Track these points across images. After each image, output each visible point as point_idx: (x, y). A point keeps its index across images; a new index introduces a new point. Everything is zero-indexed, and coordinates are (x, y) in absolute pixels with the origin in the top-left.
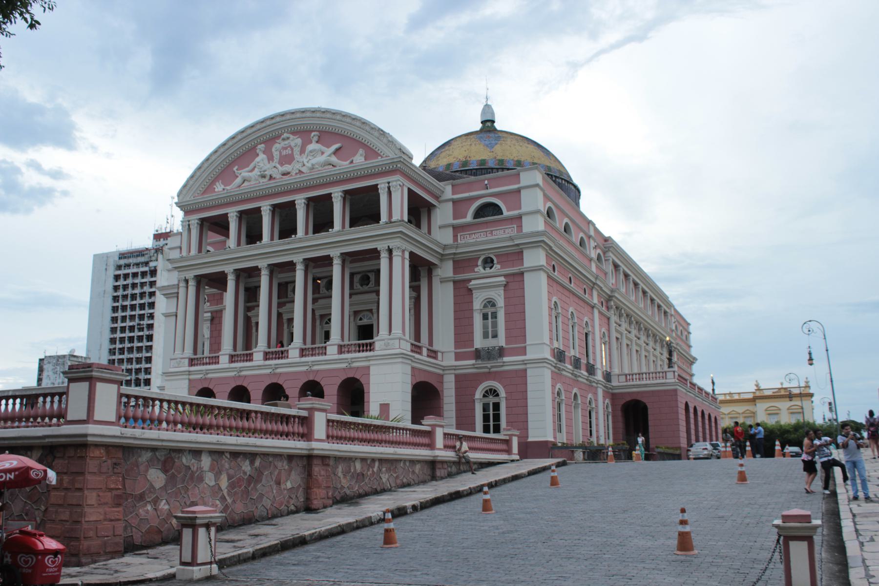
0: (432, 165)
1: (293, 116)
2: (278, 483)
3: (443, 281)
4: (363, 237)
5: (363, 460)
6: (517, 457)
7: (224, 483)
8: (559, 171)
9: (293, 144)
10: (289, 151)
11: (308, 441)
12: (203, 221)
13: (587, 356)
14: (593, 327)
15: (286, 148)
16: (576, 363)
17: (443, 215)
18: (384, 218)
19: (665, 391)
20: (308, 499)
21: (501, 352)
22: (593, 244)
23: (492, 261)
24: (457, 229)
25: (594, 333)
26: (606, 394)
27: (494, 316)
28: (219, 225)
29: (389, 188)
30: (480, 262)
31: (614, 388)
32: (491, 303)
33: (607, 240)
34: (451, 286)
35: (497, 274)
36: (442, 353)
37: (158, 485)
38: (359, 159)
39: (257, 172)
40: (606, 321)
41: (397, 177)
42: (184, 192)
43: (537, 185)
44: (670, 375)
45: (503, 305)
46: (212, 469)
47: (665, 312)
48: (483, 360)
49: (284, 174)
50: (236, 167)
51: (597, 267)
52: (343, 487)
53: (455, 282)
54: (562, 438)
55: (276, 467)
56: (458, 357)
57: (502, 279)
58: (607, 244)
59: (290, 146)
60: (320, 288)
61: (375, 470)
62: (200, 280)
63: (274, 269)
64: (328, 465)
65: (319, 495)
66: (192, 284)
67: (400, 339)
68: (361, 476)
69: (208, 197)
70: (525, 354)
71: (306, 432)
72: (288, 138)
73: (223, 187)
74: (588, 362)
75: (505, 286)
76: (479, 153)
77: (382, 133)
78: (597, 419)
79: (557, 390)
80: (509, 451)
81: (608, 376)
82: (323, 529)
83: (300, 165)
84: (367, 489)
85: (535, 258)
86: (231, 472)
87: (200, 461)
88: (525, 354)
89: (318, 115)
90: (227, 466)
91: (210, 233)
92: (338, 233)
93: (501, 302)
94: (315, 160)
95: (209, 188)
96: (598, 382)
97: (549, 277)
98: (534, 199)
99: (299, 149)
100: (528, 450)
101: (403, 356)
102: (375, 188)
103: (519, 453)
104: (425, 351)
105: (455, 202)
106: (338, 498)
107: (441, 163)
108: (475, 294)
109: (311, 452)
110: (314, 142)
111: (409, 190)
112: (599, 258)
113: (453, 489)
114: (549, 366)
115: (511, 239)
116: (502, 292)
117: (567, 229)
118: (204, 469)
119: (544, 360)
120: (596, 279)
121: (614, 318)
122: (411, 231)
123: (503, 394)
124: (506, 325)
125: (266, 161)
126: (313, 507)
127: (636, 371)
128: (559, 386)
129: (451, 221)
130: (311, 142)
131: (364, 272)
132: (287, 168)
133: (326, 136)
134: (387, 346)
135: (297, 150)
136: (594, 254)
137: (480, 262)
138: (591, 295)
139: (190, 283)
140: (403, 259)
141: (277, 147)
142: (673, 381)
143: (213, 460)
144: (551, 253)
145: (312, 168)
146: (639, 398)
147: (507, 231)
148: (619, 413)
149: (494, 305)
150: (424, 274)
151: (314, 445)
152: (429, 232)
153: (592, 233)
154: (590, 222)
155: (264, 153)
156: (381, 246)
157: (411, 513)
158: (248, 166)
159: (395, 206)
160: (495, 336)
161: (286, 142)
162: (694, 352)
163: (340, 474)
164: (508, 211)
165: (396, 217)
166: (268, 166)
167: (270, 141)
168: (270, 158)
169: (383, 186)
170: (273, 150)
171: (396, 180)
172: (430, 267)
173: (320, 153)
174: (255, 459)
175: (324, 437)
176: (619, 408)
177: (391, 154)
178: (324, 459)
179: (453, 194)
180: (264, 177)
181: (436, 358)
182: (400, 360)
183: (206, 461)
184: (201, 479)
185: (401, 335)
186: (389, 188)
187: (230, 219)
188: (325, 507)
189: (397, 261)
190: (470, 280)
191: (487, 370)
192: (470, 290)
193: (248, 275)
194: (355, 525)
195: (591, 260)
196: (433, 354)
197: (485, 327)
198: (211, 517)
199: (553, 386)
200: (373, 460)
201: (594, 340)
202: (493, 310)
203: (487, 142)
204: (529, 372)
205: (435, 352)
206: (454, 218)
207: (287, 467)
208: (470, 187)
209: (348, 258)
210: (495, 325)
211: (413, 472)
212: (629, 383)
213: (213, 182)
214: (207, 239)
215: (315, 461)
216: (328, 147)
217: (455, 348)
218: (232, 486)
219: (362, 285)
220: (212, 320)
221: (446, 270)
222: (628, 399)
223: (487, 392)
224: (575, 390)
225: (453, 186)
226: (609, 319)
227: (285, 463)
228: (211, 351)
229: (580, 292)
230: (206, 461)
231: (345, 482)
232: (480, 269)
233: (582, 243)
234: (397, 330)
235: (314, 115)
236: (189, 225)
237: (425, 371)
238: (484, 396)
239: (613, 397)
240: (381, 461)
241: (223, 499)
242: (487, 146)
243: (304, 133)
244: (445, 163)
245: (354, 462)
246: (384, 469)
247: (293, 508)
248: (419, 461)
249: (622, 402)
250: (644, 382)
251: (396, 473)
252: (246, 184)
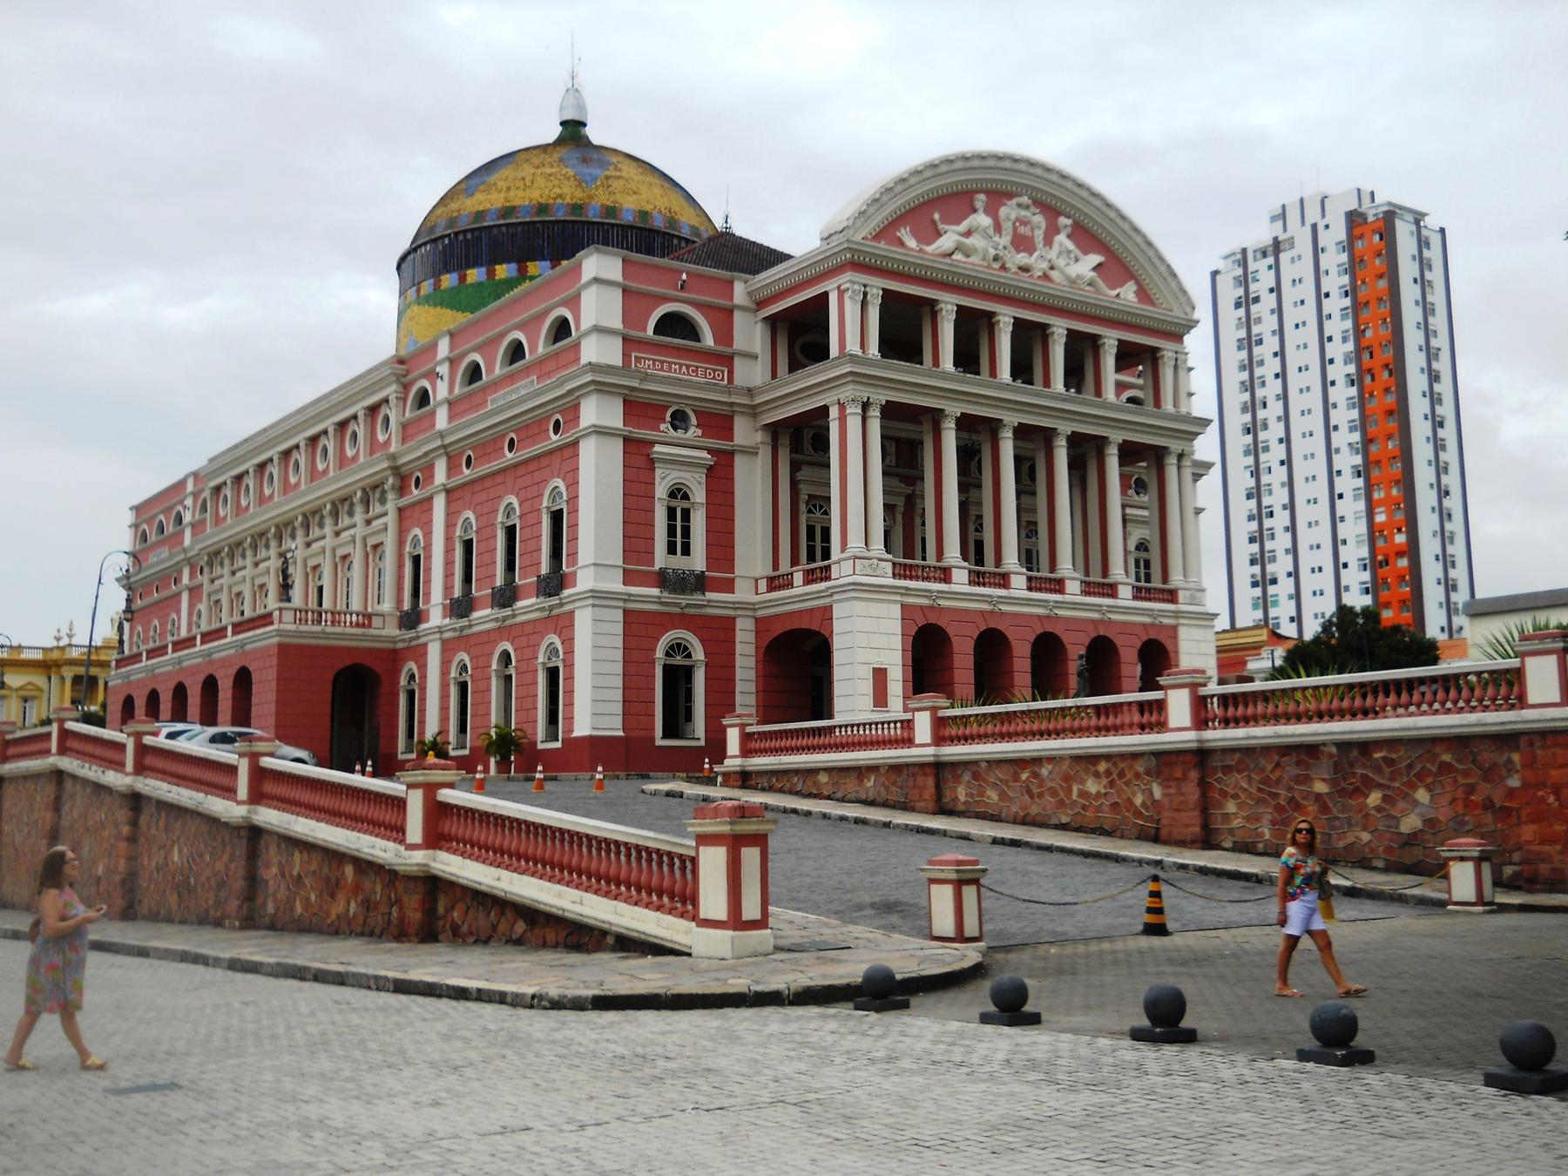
1: (1062, 182)
15: (1025, 223)
38: (1128, 292)
66: (875, 413)
72: (1027, 207)
73: (912, 243)
132: (1022, 258)
135: (1039, 235)
156: (1175, 446)
158: (958, 223)
167: (998, 196)
168: (998, 228)
216: (1086, 253)
236: (865, 294)
252: (958, 256)
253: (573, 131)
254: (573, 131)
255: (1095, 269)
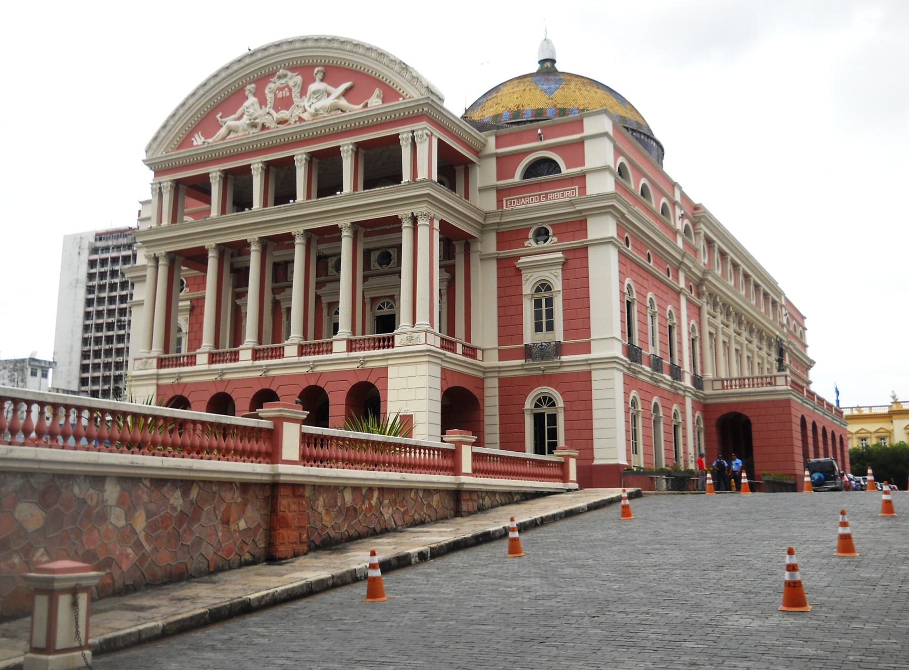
0: (476, 116)
1: (292, 46)
2: (226, 522)
3: (484, 258)
4: (379, 202)
5: (356, 489)
6: (576, 486)
7: (140, 523)
8: (638, 123)
9: (291, 84)
10: (285, 93)
11: (272, 463)
12: (177, 184)
13: (671, 355)
14: (679, 318)
15: (282, 89)
16: (656, 364)
17: (485, 174)
18: (406, 177)
19: (774, 401)
20: (271, 544)
21: (559, 349)
22: (679, 212)
23: (547, 232)
24: (502, 192)
25: (680, 326)
26: (696, 405)
27: (549, 302)
28: (197, 188)
29: (413, 138)
30: (531, 235)
31: (706, 397)
32: (544, 286)
33: (697, 208)
34: (493, 266)
35: (552, 251)
36: (483, 350)
37: (31, 527)
39: (245, 120)
40: (696, 311)
41: (424, 124)
42: (154, 146)
43: (606, 134)
44: (781, 381)
45: (560, 288)
46: (121, 503)
47: (774, 303)
48: (534, 359)
49: (282, 122)
50: (220, 114)
51: (684, 242)
52: (324, 527)
53: (499, 260)
54: (639, 461)
55: (222, 500)
56: (503, 356)
57: (560, 255)
58: (697, 214)
59: (288, 86)
60: (325, 268)
61: (373, 502)
62: (175, 259)
63: (266, 243)
64: (302, 496)
65: (287, 538)
67: (426, 332)
68: (353, 511)
69: (184, 152)
70: (589, 352)
71: (270, 450)
72: (285, 76)
73: (203, 139)
74: (672, 363)
75: (564, 264)
76: (534, 100)
77: (405, 67)
78: (685, 437)
79: (631, 398)
80: (564, 478)
81: (698, 382)
82: (279, 589)
83: (301, 110)
84: (361, 529)
85: (602, 228)
86: (152, 507)
87: (103, 491)
88: (589, 352)
89: (323, 44)
90: (145, 498)
91: (189, 200)
92: (348, 197)
93: (558, 285)
94: (320, 103)
95: (186, 141)
96: (686, 389)
97: (621, 253)
98: (600, 154)
99: (299, 90)
100: (592, 476)
101: (430, 353)
102: (395, 139)
103: (579, 480)
104: (459, 348)
105: (499, 158)
106: (318, 543)
107: (486, 114)
108: (525, 275)
109: (277, 478)
110: (317, 80)
111: (439, 140)
112: (687, 230)
113: (480, 530)
114: (621, 368)
115: (571, 203)
116: (560, 272)
117: (644, 192)
118: (109, 503)
119: (613, 360)
120: (683, 256)
121: (706, 308)
122: (442, 194)
123: (560, 403)
124: (564, 313)
125: (257, 106)
126: (278, 555)
127: (735, 375)
128: (633, 393)
129: (493, 181)
130: (314, 81)
131: (381, 247)
132: (284, 114)
133: (333, 72)
134: (410, 341)
135: (296, 92)
136: (679, 225)
137: (531, 235)
138: (677, 278)
139: (161, 262)
140: (431, 229)
141: (270, 88)
142: (784, 388)
143: (123, 490)
144: (623, 225)
145: (316, 114)
146: (739, 410)
147: (566, 194)
148: (714, 430)
149: (549, 289)
150: (459, 249)
151: (282, 468)
152: (467, 196)
153: (678, 198)
154: (674, 185)
155: (255, 95)
156: (403, 212)
157: (417, 563)
158: (234, 113)
159: (421, 161)
160: (550, 327)
161: (283, 81)
162: (811, 353)
163: (321, 509)
164: (567, 168)
165: (422, 175)
166: (260, 112)
167: (261, 80)
168: (263, 102)
169: (405, 135)
170: (267, 91)
171: (422, 128)
172: (467, 241)
173: (325, 95)
174: (190, 489)
175: (296, 457)
176: (714, 422)
177: (414, 94)
178: (296, 488)
179: (497, 147)
180: (254, 126)
181: (474, 357)
182: (426, 359)
183: (112, 492)
184: (103, 517)
185: (428, 327)
186: (413, 138)
187: (212, 181)
188: (296, 555)
189: (423, 232)
190: (518, 257)
191: (540, 372)
192: (519, 271)
193: (233, 253)
194: (330, 582)
195: (675, 233)
196: (470, 351)
197: (538, 315)
198: (80, 578)
199: (626, 394)
200: (371, 489)
201: (680, 335)
202: (547, 294)
203: (545, 87)
204: (595, 375)
205: (474, 350)
206: (499, 179)
207: (240, 500)
208: (518, 138)
209: (361, 229)
210: (550, 314)
211: (429, 506)
212: (726, 391)
213: (191, 134)
214: (184, 208)
215: (282, 491)
216: (336, 85)
217: (500, 344)
218: (152, 527)
219: (381, 265)
220: (192, 309)
221: (490, 245)
222: (725, 411)
223: (539, 400)
224: (655, 399)
225: (497, 137)
226: (700, 308)
227: (237, 494)
228: (189, 349)
229: (662, 274)
230: (112, 492)
231: (328, 521)
232: (531, 243)
233: (664, 210)
234: (423, 319)
235: (318, 44)
236: (160, 188)
237: (459, 373)
238: (536, 406)
239: (705, 408)
240: (381, 489)
241: (138, 545)
242: (545, 91)
243: (305, 69)
244: (492, 114)
245: (342, 492)
246: (386, 502)
247: (247, 557)
248: (437, 491)
249: (719, 415)
250: (747, 390)
251: (403, 506)
252: (232, 135)
253: (548, 68)
254: (548, 68)
255: (345, 94)
